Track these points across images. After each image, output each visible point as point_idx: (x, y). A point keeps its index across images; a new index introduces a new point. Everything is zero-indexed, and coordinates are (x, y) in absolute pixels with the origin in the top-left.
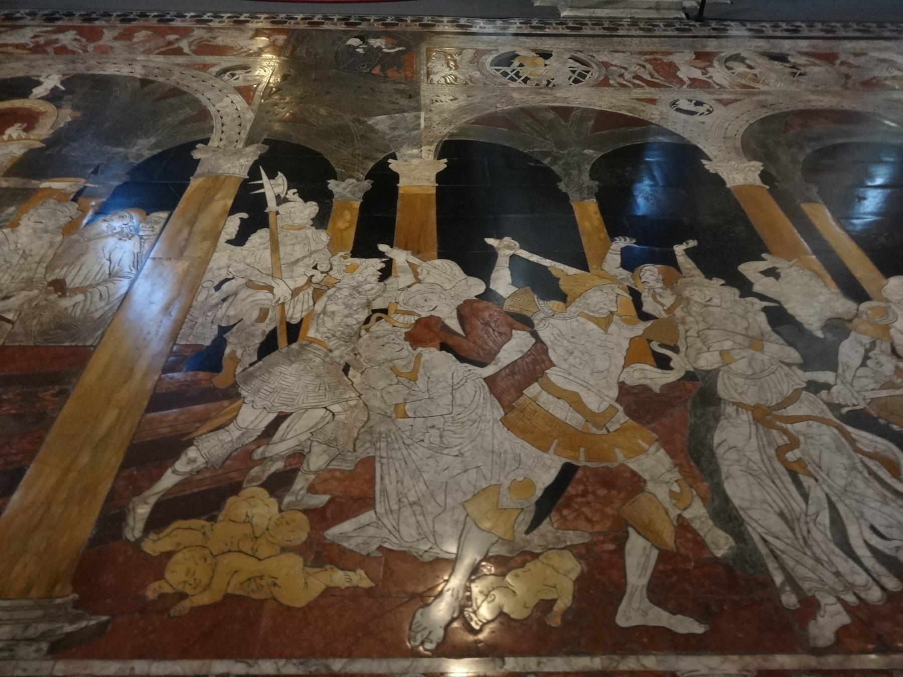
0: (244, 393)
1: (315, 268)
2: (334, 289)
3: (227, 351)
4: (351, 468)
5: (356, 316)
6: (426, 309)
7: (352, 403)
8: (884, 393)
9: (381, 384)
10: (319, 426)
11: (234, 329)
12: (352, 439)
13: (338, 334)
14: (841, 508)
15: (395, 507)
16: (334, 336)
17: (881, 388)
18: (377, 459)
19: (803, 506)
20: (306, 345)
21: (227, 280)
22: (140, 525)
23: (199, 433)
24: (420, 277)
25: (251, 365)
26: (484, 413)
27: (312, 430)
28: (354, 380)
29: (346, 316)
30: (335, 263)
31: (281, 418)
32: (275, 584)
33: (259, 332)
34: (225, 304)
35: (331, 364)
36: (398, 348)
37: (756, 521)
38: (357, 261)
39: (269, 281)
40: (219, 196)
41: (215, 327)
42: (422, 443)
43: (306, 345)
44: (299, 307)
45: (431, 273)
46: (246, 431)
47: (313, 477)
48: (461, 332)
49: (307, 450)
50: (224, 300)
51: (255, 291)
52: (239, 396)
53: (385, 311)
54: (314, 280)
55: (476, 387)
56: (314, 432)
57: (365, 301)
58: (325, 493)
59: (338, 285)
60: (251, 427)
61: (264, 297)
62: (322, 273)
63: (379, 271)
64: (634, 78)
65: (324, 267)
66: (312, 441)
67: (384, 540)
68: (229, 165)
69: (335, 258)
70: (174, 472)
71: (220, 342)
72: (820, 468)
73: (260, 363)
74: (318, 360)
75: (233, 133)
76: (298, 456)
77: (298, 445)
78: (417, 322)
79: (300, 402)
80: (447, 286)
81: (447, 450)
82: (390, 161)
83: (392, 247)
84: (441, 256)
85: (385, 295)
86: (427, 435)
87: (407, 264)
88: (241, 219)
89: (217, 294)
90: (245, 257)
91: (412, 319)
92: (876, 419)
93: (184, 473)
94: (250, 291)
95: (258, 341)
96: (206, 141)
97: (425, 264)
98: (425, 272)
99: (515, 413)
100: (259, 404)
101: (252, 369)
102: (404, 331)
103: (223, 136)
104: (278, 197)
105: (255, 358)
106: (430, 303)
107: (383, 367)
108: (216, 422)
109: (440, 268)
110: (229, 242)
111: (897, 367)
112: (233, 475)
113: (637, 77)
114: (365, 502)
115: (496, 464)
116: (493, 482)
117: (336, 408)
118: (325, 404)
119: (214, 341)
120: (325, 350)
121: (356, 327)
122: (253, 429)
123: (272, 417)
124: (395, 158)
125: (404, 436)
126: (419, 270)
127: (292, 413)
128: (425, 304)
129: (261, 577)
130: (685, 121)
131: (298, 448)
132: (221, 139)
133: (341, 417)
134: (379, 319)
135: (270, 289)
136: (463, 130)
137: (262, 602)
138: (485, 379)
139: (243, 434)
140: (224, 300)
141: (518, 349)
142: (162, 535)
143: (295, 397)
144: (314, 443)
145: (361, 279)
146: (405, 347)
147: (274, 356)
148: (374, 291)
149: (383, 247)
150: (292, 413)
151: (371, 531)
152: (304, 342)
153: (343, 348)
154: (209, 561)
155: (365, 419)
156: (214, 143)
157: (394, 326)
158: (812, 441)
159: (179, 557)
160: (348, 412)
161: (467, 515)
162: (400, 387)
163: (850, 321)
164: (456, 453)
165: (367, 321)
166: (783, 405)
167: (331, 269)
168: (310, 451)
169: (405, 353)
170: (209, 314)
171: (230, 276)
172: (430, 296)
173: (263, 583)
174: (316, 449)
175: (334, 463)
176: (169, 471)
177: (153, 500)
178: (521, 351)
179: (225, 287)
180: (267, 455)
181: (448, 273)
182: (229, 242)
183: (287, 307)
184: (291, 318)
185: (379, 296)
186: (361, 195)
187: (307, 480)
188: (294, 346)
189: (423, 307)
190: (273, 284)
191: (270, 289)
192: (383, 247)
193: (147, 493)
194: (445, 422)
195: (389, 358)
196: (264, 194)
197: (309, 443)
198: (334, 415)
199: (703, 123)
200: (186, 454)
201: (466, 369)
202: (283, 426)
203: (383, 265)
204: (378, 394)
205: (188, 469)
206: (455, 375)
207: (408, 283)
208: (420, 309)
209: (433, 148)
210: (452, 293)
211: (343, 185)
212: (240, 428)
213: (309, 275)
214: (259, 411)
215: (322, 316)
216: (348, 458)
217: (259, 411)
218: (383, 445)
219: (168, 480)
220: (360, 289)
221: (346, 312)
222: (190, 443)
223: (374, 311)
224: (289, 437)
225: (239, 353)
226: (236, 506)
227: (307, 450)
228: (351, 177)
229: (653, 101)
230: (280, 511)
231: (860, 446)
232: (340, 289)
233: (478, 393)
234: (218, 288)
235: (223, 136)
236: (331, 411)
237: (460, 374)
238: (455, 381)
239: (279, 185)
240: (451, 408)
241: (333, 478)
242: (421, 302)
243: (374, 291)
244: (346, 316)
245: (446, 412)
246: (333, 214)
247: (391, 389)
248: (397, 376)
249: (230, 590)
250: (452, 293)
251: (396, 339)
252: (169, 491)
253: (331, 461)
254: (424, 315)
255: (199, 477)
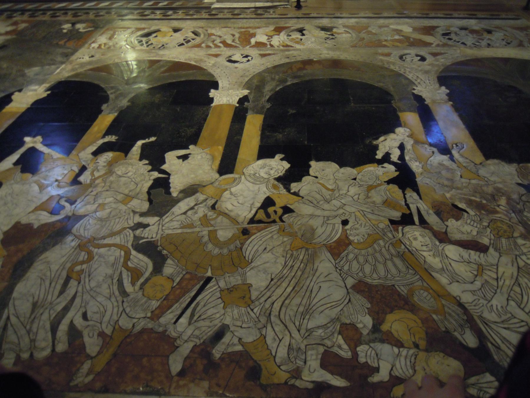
8: (179, 231)
14: (78, 300)
17: (181, 228)
19: (55, 297)
37: (14, 306)
64: (220, 42)
72: (89, 276)
92: (158, 246)
111: (205, 216)
113: (224, 43)
130: (226, 67)
136: (77, 75)
158: (102, 259)
163: (204, 186)
166: (104, 238)
199: (236, 68)
229: (217, 56)
231: (129, 263)
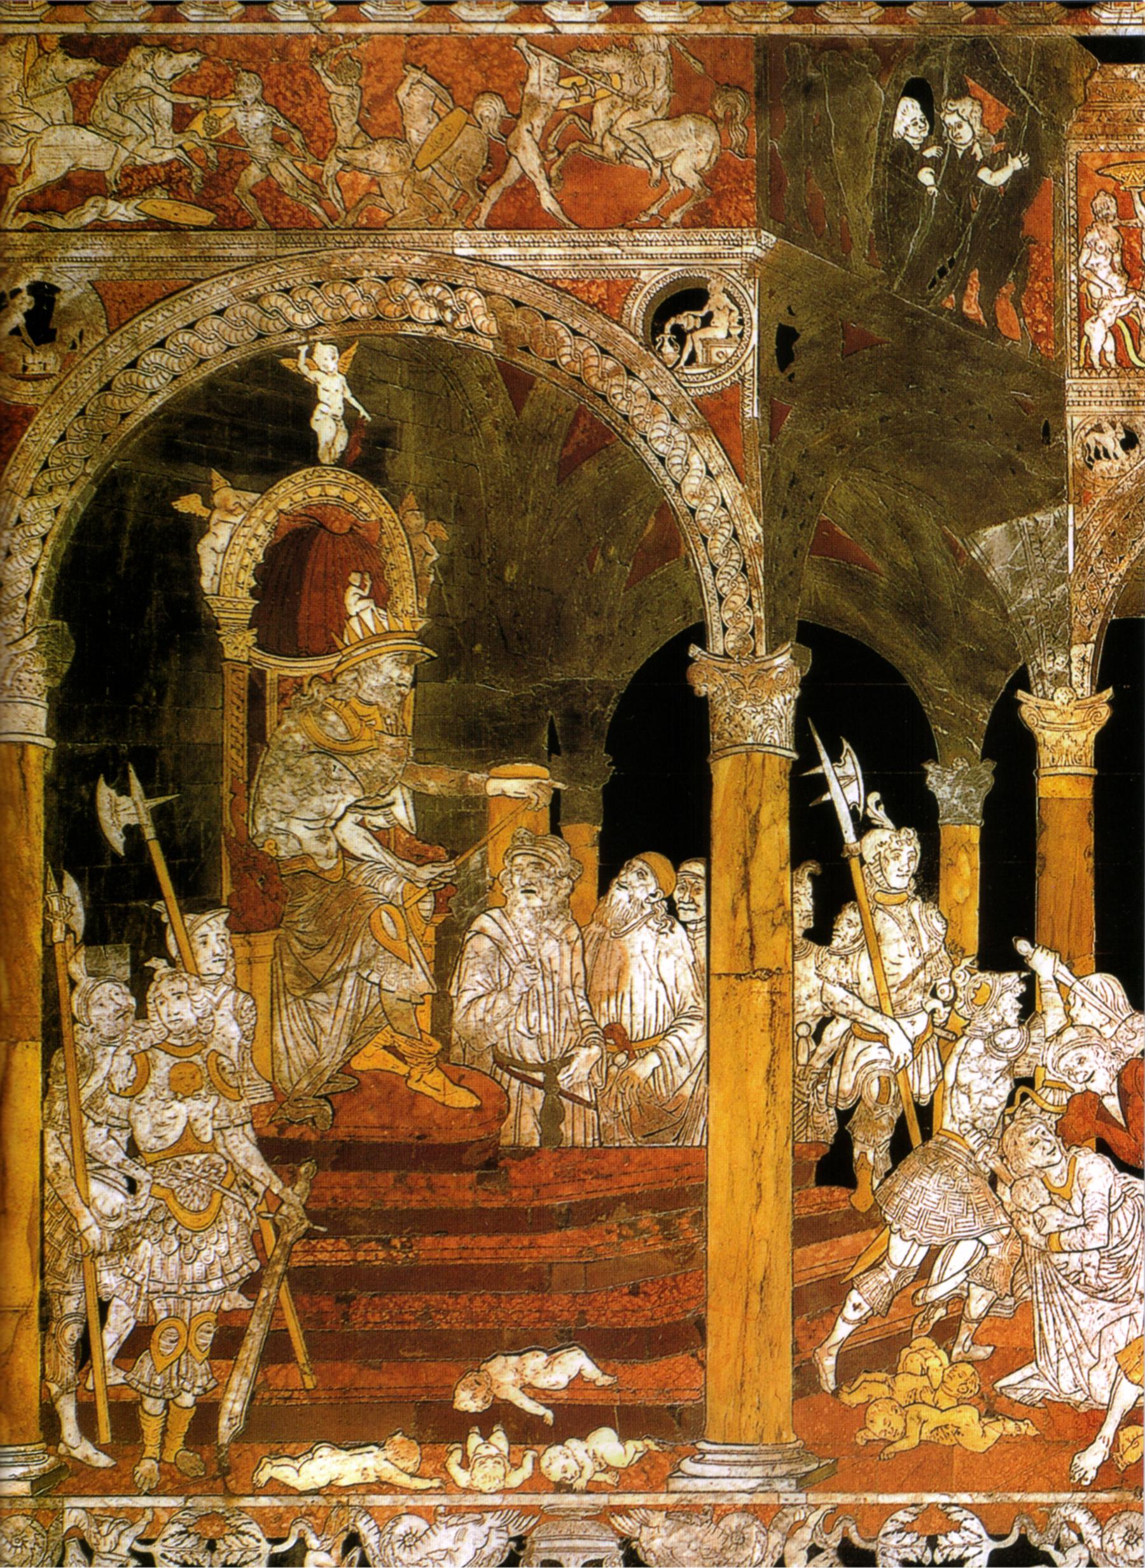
2: (964, 1039)
15: (1054, 1359)
22: (831, 1377)
31: (933, 1253)
46: (902, 1271)
48: (1121, 1120)
56: (969, 1269)
60: (906, 1264)
65: (946, 993)
71: (843, 1142)
76: (960, 1299)
88: (812, 876)
94: (860, 1045)
105: (890, 1165)
108: (869, 1260)
114: (1026, 1356)
128: (1079, 1069)
129: (946, 1426)
147: (912, 1161)
149: (1023, 946)
153: (987, 1148)
165: (1010, 1101)
174: (976, 1292)
184: (920, 1096)
188: (931, 1144)
193: (827, 1344)
196: (831, 803)
197: (965, 1285)
212: (894, 1267)
219: (842, 1330)
222: (851, 1286)
224: (946, 1276)
226: (912, 1360)
230: (951, 1363)
245: (1101, 1244)
249: (924, 1437)
252: (844, 1342)
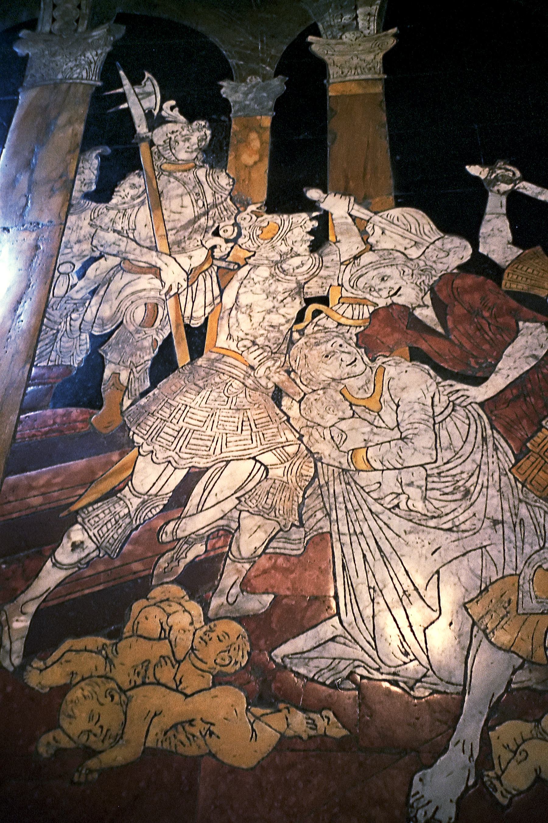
0: (137, 439)
1: (216, 233)
2: (248, 267)
3: (107, 373)
4: (299, 552)
5: (282, 311)
6: (384, 293)
7: (291, 450)
9: (330, 419)
10: (248, 488)
11: (112, 339)
12: (296, 507)
13: (260, 341)
16: (254, 343)
18: (335, 536)
20: (217, 360)
21: (94, 260)
22: (18, 646)
23: (84, 502)
24: (371, 240)
25: (144, 394)
26: (485, 459)
27: (238, 495)
28: (290, 413)
29: (269, 312)
30: (245, 224)
32: (211, 733)
33: (147, 343)
34: (95, 300)
35: (256, 390)
36: (348, 359)
38: (276, 218)
39: (153, 258)
40: (62, 120)
41: (85, 336)
42: (397, 511)
43: (217, 360)
44: (200, 300)
45: (386, 232)
47: (247, 566)
48: (440, 329)
49: (234, 525)
50: (93, 293)
51: (135, 276)
52: (131, 444)
53: (324, 300)
54: (217, 253)
55: (468, 418)
57: (294, 285)
58: (266, 592)
59: (251, 261)
61: (148, 286)
62: (227, 241)
63: (311, 233)
65: (230, 232)
66: (241, 511)
67: (357, 663)
68: (70, 64)
69: (244, 215)
70: (56, 564)
73: (156, 391)
74: (236, 384)
75: (69, 6)
77: (222, 518)
78: (373, 315)
79: (218, 451)
80: (414, 253)
81: (434, 520)
82: (310, 38)
83: (325, 191)
84: (398, 205)
85: (323, 273)
86: (403, 497)
87: (350, 220)
89: (81, 283)
90: (113, 221)
91: (367, 311)
93: (72, 565)
94: (128, 277)
95: (148, 356)
96: (32, 25)
97: (376, 218)
98: (378, 231)
99: (532, 459)
100: (161, 455)
101: (144, 401)
102: (354, 331)
103: (56, 14)
104: (149, 114)
105: (148, 384)
106: (390, 283)
107: (331, 391)
108: (105, 487)
109: (399, 223)
110: (88, 196)
112: (137, 566)
115: (510, 542)
116: (509, 571)
117: (268, 458)
118: (254, 453)
119: (88, 359)
120: (245, 368)
121: (285, 329)
122: (156, 495)
123: (180, 475)
124: (318, 34)
125: (369, 499)
126: (369, 230)
127: (208, 469)
128: (383, 285)
129: (191, 722)
131: (221, 522)
132: (54, 20)
133: (277, 473)
134: (317, 313)
135: (156, 271)
137: (196, 760)
138: (481, 405)
139: (143, 502)
140: (93, 293)
141: (528, 353)
142: (49, 661)
143: (209, 443)
144: (244, 514)
145: (284, 249)
146: (359, 357)
148: (305, 268)
149: (313, 194)
150: (208, 469)
151: (336, 649)
152: (213, 356)
153: (269, 363)
154: (117, 698)
155: (311, 473)
156: (45, 27)
157: (339, 324)
159: (77, 693)
160: (287, 464)
161: (474, 624)
162: (357, 422)
164: (449, 525)
167: (239, 234)
168: (239, 527)
169: (360, 367)
170: (74, 316)
171: (97, 254)
172: (388, 271)
173: (195, 731)
175: (274, 544)
176: (49, 564)
177: (32, 608)
178: (534, 356)
179: (91, 272)
180: (180, 534)
181: (413, 231)
182: (88, 196)
183: (182, 299)
185: (314, 276)
186: (271, 104)
187: (238, 571)
189: (380, 290)
190: (159, 264)
191: (156, 271)
192: (313, 194)
193: (23, 598)
194: (428, 476)
195: (336, 376)
196: (128, 110)
197: (236, 514)
198: (267, 469)
200: (69, 537)
201: (451, 389)
202: (198, 489)
203: (316, 224)
204: (327, 432)
205: (75, 557)
206: (436, 399)
207: (355, 252)
208: (375, 294)
209: (375, 9)
210: (422, 263)
211: (243, 88)
212: (138, 495)
213: (209, 245)
214: (163, 466)
215: (234, 312)
216: (294, 537)
217: (163, 466)
218: (342, 514)
220: (285, 266)
221: (269, 304)
223: (309, 301)
225: (124, 376)
227: (234, 525)
228: (254, 73)
230: (207, 620)
232: (256, 267)
233: (473, 427)
234: (82, 274)
235: (56, 14)
236: (262, 464)
237: (444, 398)
238: (438, 410)
239: (149, 94)
240: (434, 453)
241: (275, 567)
242: (376, 282)
243: (305, 268)
244: (269, 312)
245: (428, 460)
246: (233, 140)
247: (343, 425)
248: (351, 405)
250: (422, 263)
251: (345, 345)
252: (51, 594)
253: (270, 541)
254: (382, 303)
255: (89, 572)
